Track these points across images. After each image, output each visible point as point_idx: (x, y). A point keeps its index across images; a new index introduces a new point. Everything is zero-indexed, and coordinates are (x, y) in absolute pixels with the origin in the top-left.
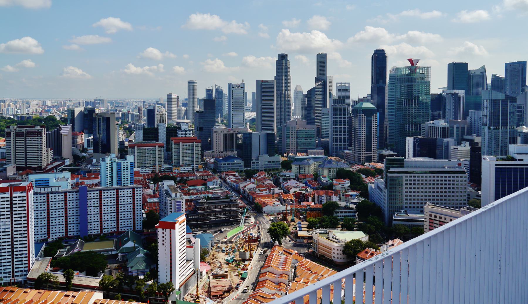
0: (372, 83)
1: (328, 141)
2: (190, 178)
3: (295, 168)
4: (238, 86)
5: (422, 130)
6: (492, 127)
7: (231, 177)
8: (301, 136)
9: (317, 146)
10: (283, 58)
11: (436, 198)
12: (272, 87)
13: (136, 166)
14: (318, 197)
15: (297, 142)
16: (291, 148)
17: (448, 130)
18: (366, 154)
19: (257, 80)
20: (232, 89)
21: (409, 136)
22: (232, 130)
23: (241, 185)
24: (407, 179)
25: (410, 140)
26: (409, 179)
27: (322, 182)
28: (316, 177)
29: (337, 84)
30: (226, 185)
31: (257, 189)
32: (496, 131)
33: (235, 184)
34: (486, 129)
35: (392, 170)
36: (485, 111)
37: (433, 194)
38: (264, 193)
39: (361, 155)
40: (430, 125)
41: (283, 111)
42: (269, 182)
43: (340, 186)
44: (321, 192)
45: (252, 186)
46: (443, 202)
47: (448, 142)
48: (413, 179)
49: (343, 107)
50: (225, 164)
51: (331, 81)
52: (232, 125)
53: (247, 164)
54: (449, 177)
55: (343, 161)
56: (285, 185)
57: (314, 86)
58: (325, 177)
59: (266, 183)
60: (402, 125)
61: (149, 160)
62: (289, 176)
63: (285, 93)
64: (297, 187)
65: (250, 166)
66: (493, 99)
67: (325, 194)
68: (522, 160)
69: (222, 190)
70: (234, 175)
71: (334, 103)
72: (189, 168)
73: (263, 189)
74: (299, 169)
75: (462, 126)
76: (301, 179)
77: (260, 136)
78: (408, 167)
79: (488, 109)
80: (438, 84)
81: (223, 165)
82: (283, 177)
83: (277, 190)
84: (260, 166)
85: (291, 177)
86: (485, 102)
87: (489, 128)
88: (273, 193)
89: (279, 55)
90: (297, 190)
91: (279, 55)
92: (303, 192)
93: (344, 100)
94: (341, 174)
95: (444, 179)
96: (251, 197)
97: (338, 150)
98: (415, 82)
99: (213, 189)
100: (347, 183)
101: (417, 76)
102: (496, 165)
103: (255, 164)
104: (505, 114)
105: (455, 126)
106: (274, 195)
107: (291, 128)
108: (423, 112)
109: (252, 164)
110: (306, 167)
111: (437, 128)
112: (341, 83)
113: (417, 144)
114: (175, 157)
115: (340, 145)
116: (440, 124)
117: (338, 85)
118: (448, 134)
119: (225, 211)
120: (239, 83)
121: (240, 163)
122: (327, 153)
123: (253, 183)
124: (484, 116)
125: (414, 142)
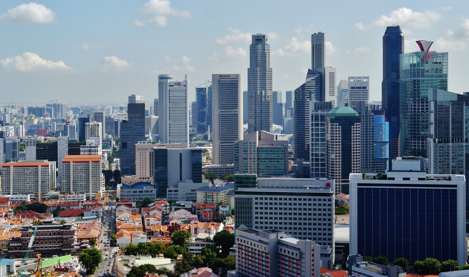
1: (309, 164)
2: (71, 207)
4: (179, 84)
6: (437, 140)
8: (263, 156)
10: (259, 40)
13: (11, 192)
15: (258, 165)
18: (342, 182)
24: (257, 201)
26: (259, 201)
34: (431, 140)
35: (240, 189)
37: (290, 221)
46: (293, 231)
48: (264, 201)
51: (332, 75)
52: (168, 139)
54: (295, 199)
57: (304, 82)
61: (29, 184)
62: (184, 206)
63: (261, 93)
68: (393, 179)
71: (315, 109)
72: (81, 195)
74: (206, 196)
76: (198, 210)
77: (181, 154)
81: (126, 193)
82: (176, 207)
84: (179, 196)
87: (434, 141)
98: (423, 76)
99: (86, 220)
102: (359, 185)
103: (173, 193)
104: (458, 122)
107: (249, 145)
109: (168, 193)
110: (215, 194)
114: (65, 181)
119: (57, 239)
120: (181, 80)
121: (151, 191)
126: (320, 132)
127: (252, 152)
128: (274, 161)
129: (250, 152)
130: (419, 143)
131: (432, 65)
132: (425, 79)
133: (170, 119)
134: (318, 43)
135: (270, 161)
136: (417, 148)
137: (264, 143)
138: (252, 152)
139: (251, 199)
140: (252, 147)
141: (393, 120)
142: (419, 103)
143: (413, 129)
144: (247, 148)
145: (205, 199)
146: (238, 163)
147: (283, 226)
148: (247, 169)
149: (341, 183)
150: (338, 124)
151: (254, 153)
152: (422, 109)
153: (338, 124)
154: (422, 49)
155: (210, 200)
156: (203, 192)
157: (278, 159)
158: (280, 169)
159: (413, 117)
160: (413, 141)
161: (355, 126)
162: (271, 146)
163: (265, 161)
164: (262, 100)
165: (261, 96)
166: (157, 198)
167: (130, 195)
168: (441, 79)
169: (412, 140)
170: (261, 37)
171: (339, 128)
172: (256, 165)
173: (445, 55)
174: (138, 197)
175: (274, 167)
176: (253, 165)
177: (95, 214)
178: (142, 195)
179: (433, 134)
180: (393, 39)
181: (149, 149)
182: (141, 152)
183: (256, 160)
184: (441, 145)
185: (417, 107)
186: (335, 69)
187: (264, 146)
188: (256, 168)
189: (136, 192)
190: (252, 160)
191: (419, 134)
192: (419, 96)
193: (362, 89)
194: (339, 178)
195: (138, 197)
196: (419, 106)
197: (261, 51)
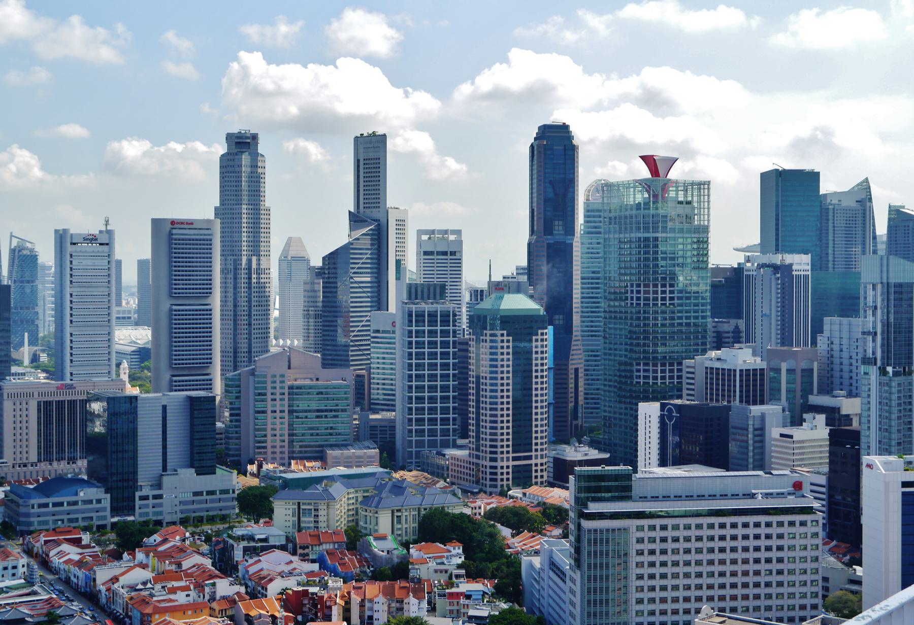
0: (532, 232)
1: (393, 421)
3: (283, 511)
5: (684, 381)
6: (890, 369)
7: (65, 547)
8: (303, 405)
9: (357, 438)
10: (242, 144)
11: (728, 592)
12: (208, 242)
14: (362, 605)
15: (291, 425)
16: (269, 444)
17: (762, 380)
18: (514, 459)
19: (153, 220)
20: (70, 249)
21: (646, 399)
22: (71, 387)
23: (103, 575)
25: (649, 413)
27: (374, 556)
28: (354, 539)
29: (420, 232)
30: (50, 577)
31: (158, 587)
32: (902, 379)
33: (81, 573)
34: (873, 371)
35: (594, 507)
36: (871, 318)
38: (181, 598)
39: (499, 464)
40: (709, 364)
41: (243, 321)
42: (197, 559)
43: (432, 565)
44: (372, 589)
45: (138, 576)
47: (763, 417)
48: (658, 534)
49: (439, 307)
50: (46, 505)
52: (68, 370)
53: (123, 502)
55: (442, 484)
56: (252, 570)
58: (383, 538)
59: (186, 564)
60: (626, 364)
62: (265, 540)
63: (249, 261)
64: (291, 573)
65: (131, 510)
66: (892, 281)
67: (385, 595)
69: (35, 593)
70: (77, 542)
71: (410, 297)
73: (176, 584)
74: (299, 513)
75: (804, 365)
76: (303, 548)
77: (164, 408)
78: (644, 498)
79: (879, 312)
80: (734, 236)
81: (36, 510)
83: (225, 587)
84: (166, 509)
85: (272, 542)
86: (870, 293)
87: (883, 372)
88: (213, 598)
89: (229, 137)
90: (292, 584)
91: (229, 137)
92: (312, 590)
93: (443, 287)
94: (435, 528)
95: (751, 531)
96: (136, 614)
97: (426, 451)
98: (665, 229)
100: (455, 555)
101: (669, 209)
103: (151, 502)
105: (784, 367)
106: (214, 605)
107: (269, 380)
108: (688, 324)
109: (138, 503)
110: (322, 507)
111: (731, 373)
112: (433, 232)
113: (670, 424)
115: (432, 433)
116: (740, 362)
117: (425, 237)
118: (762, 390)
121: (99, 501)
122: (390, 458)
123: (143, 566)
124: (869, 333)
125: (662, 417)
126: (426, 350)
127: (278, 397)
128: (326, 417)
129: (273, 397)
130: (655, 371)
131: (660, 207)
132: (669, 235)
133: (71, 322)
134: (370, 156)
135: (318, 417)
136: (651, 381)
137: (298, 376)
138: (278, 397)
139: (626, 530)
140: (278, 385)
141: (557, 322)
142: (656, 286)
143: (642, 342)
144: (265, 388)
145: (296, 519)
146: (239, 421)
147: (705, 593)
148: (265, 436)
149: (511, 463)
150: (505, 332)
151: (281, 400)
152: (663, 299)
153: (505, 332)
154: (654, 171)
155: (309, 522)
156: (291, 502)
157: (335, 411)
158: (339, 434)
159: (642, 316)
160: (642, 367)
161: (539, 337)
162: (315, 382)
163: (306, 417)
164: (250, 278)
165: (249, 268)
166: (112, 516)
167: (46, 514)
168: (697, 235)
169: (639, 364)
170: (248, 138)
171: (508, 341)
172: (286, 426)
173: (703, 186)
174: (66, 517)
175: (327, 429)
176: (278, 426)
177: (10, 571)
178: (76, 512)
179: (879, 355)
180: (554, 151)
181: (36, 395)
182: (18, 403)
183: (286, 414)
184: (897, 380)
185: (651, 296)
186: (406, 211)
187: (299, 383)
188: (286, 432)
189: (46, 505)
190: (278, 415)
191: (655, 352)
192: (655, 273)
193: (449, 257)
194: (508, 452)
195: (66, 517)
196: (656, 292)
197: (249, 169)
